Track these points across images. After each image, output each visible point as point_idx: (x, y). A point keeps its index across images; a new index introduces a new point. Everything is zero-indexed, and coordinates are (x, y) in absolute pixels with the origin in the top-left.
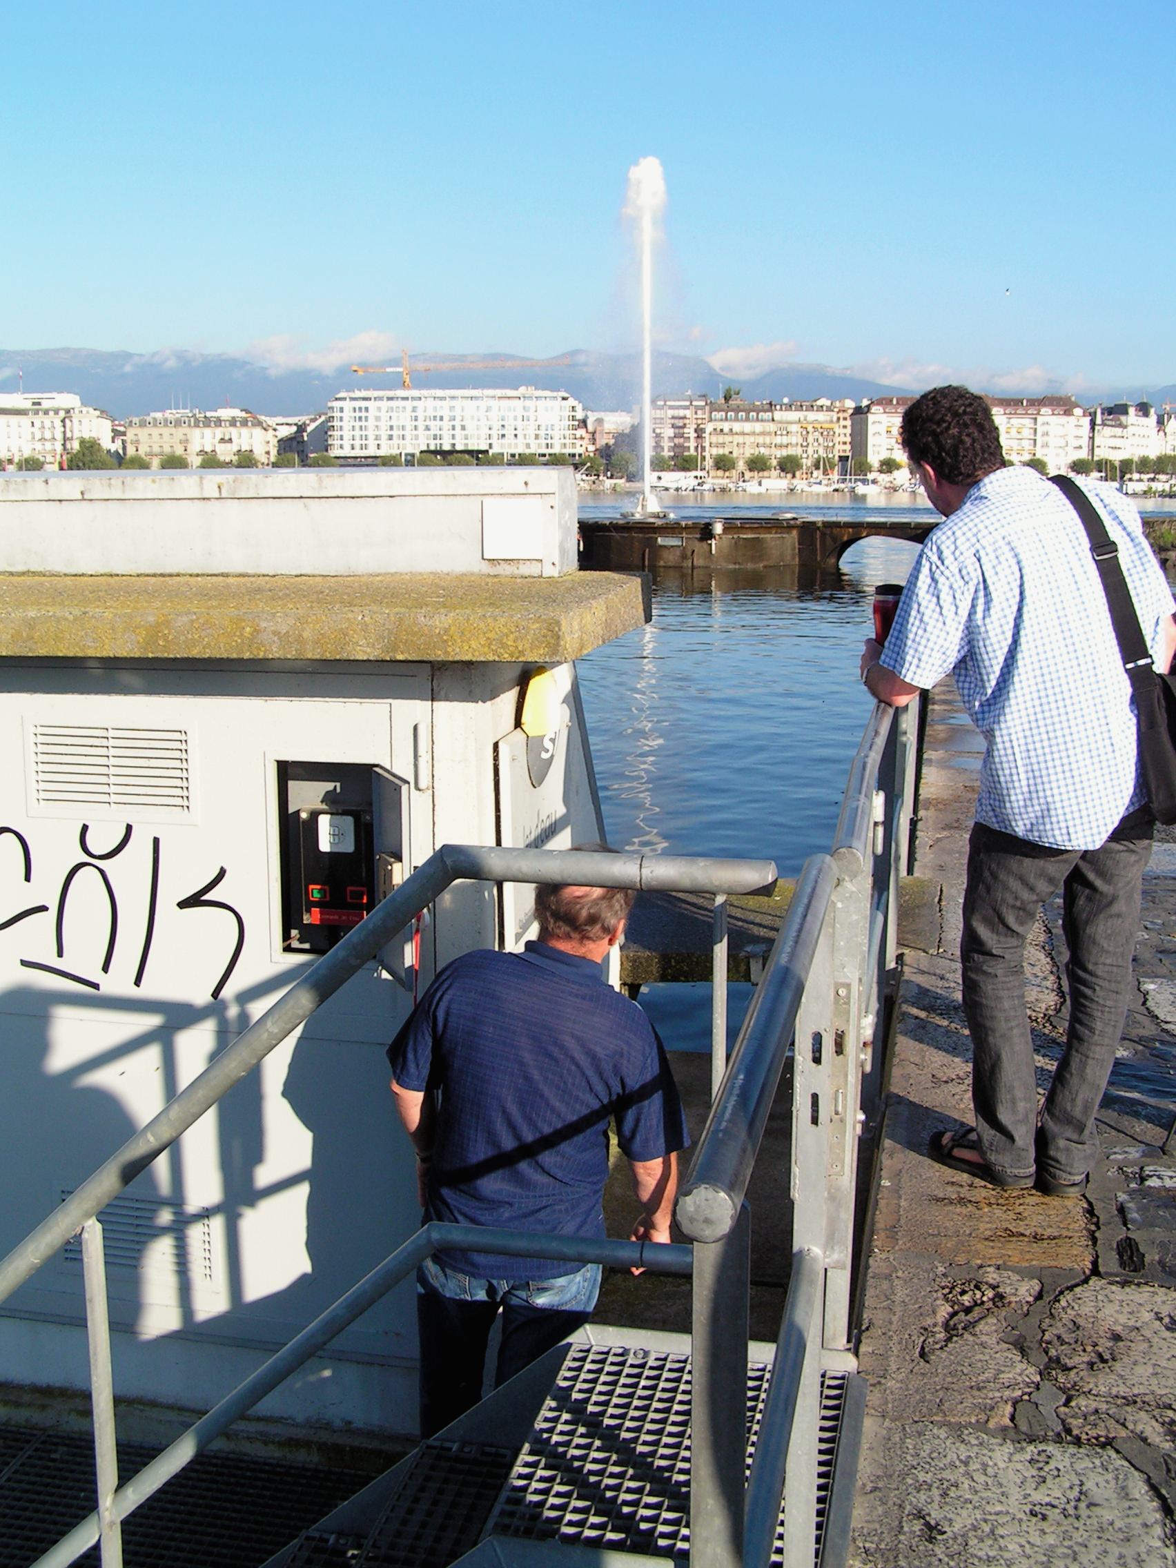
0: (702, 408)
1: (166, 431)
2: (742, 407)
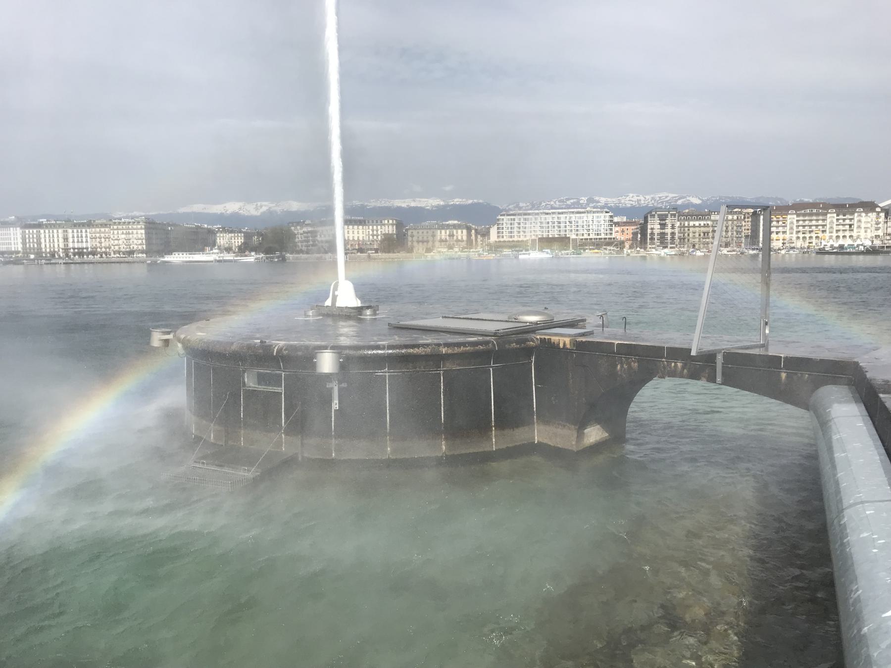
0: (674, 215)
1: (425, 231)
2: (695, 214)
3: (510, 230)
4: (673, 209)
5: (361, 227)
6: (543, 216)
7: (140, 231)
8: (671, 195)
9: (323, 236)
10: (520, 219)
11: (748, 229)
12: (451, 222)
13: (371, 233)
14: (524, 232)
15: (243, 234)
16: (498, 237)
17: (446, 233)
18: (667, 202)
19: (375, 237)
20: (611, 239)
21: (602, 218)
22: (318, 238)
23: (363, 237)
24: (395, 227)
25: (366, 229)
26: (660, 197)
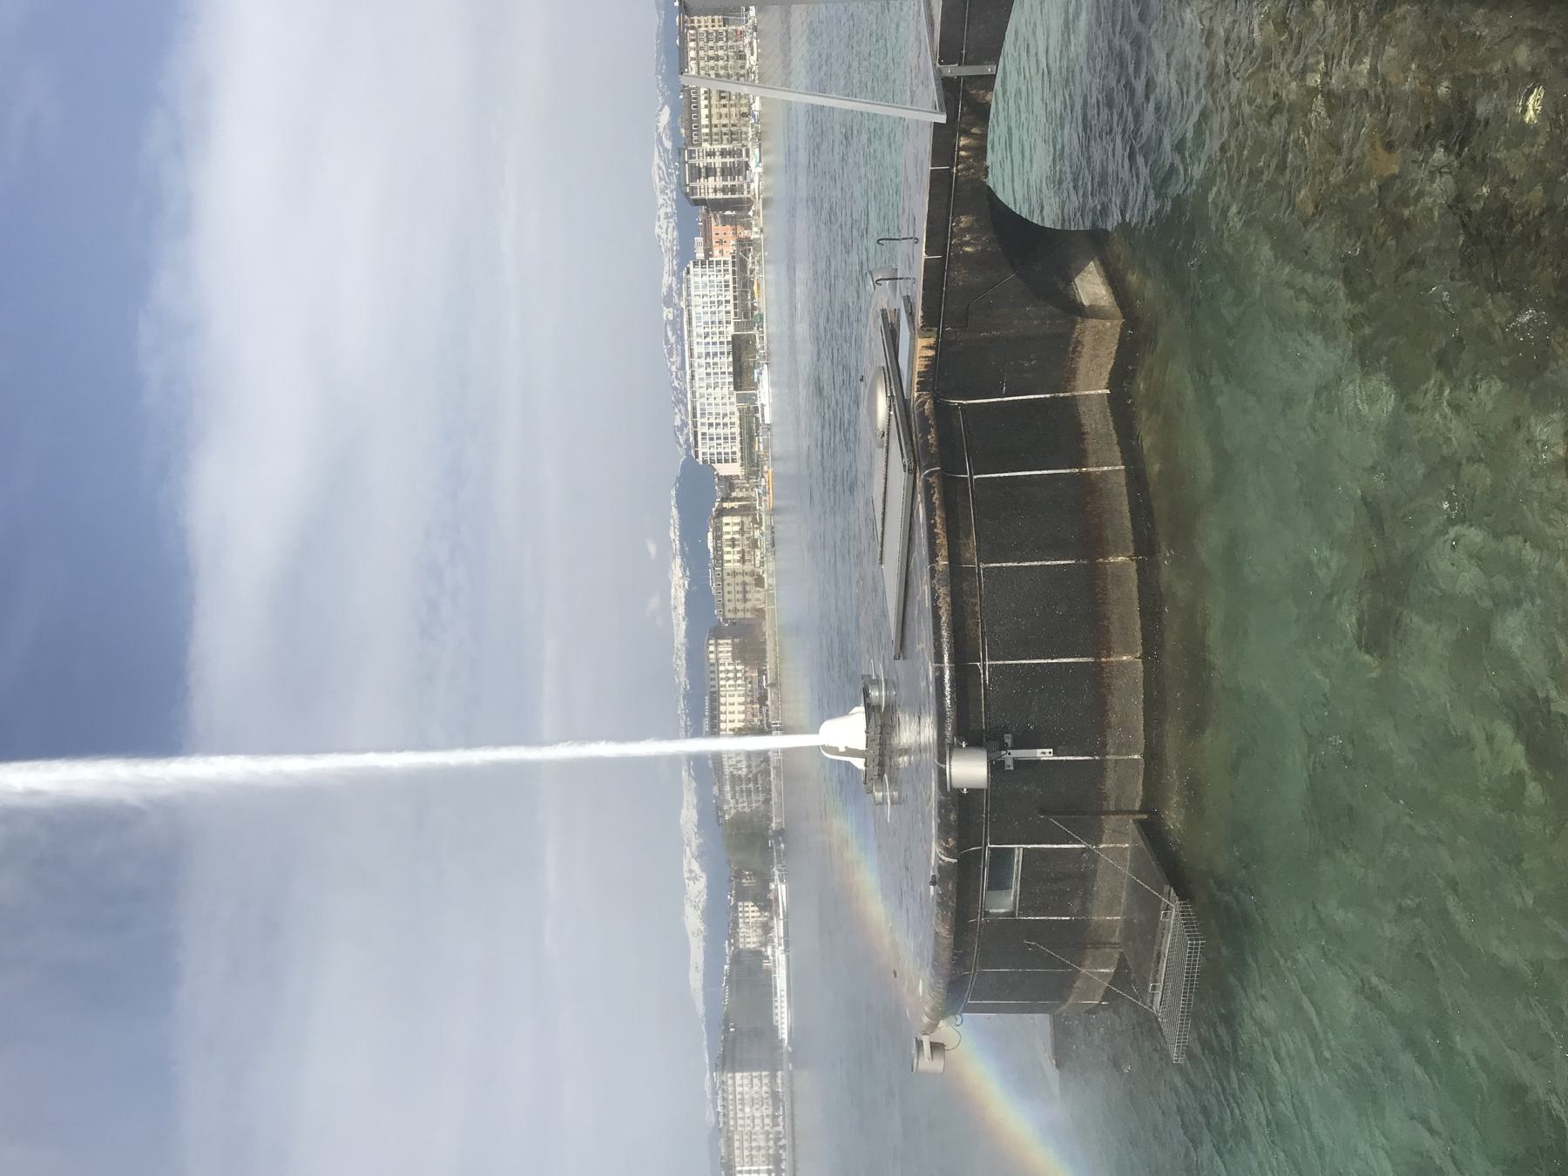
0: (691, 152)
1: (727, 589)
2: (687, 117)
3: (722, 441)
4: (680, 154)
5: (722, 700)
6: (697, 384)
7: (738, 1081)
8: (657, 160)
9: (739, 765)
10: (703, 424)
11: (713, 21)
12: (710, 545)
13: (731, 682)
14: (725, 415)
15: (740, 904)
16: (734, 461)
17: (728, 553)
18: (667, 167)
19: (739, 675)
20: (733, 262)
21: (699, 279)
22: (744, 772)
23: (739, 696)
24: (720, 641)
25: (727, 691)
26: (661, 179)
